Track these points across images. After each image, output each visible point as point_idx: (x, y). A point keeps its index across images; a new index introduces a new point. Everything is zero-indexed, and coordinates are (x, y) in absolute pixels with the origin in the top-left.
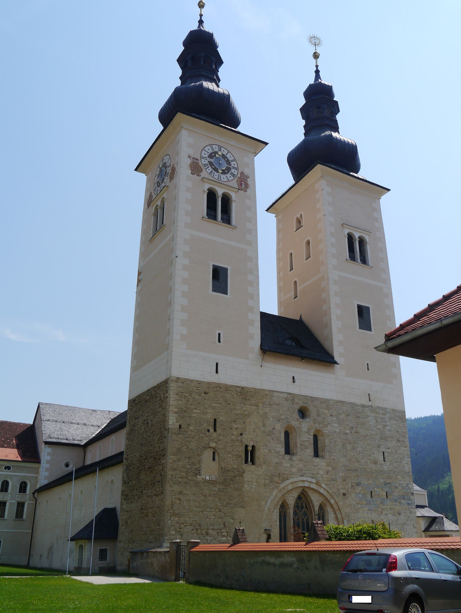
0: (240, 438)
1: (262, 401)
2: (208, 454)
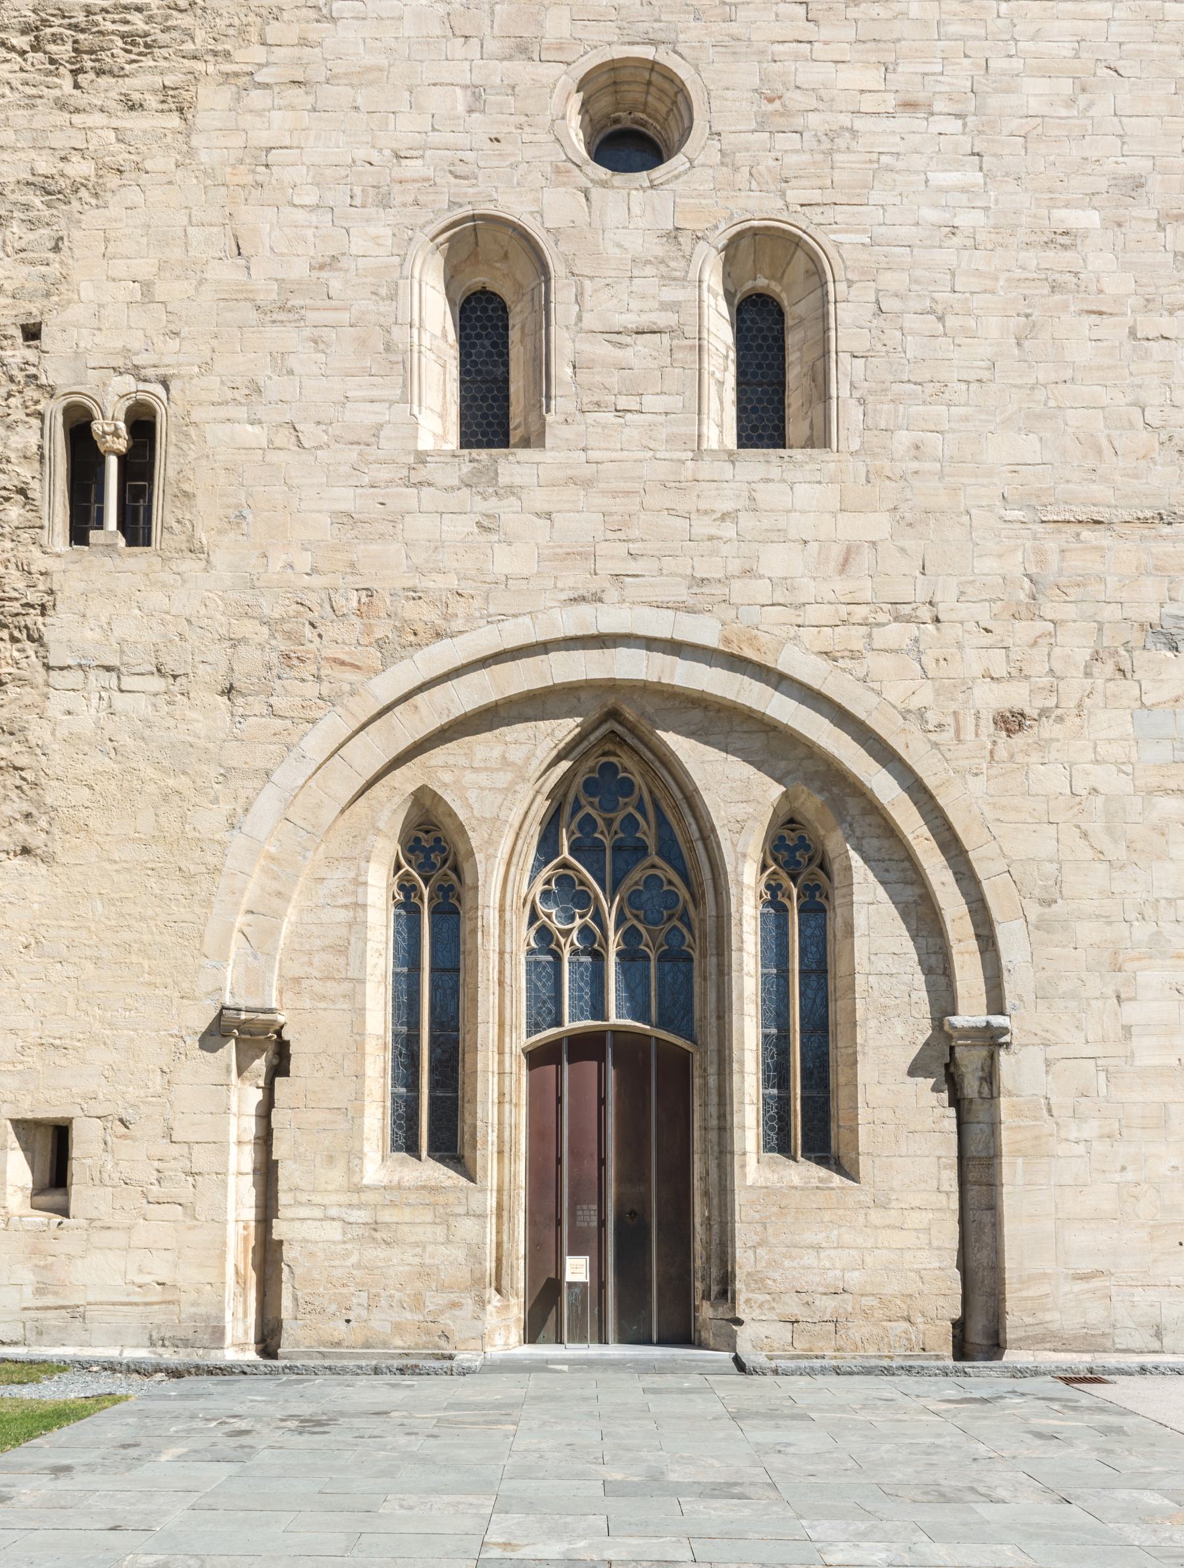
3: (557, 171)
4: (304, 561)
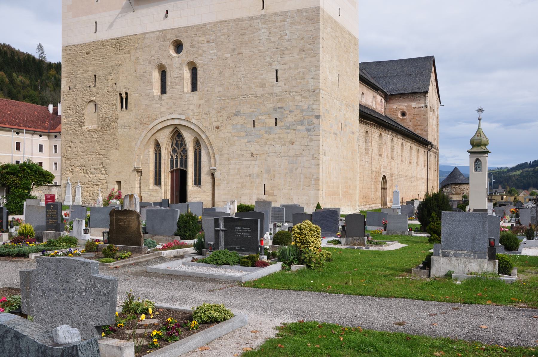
1: (135, 47)
3: (168, 56)
4: (142, 111)
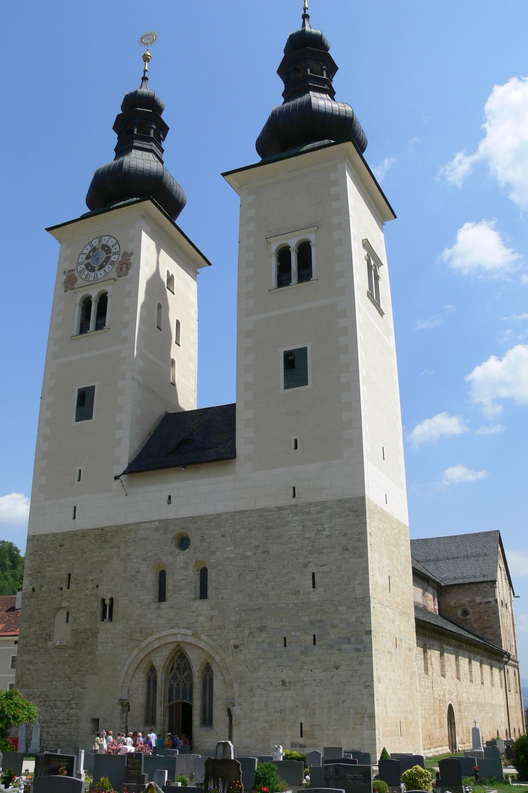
0: (94, 592)
1: (125, 540)
2: (61, 616)
